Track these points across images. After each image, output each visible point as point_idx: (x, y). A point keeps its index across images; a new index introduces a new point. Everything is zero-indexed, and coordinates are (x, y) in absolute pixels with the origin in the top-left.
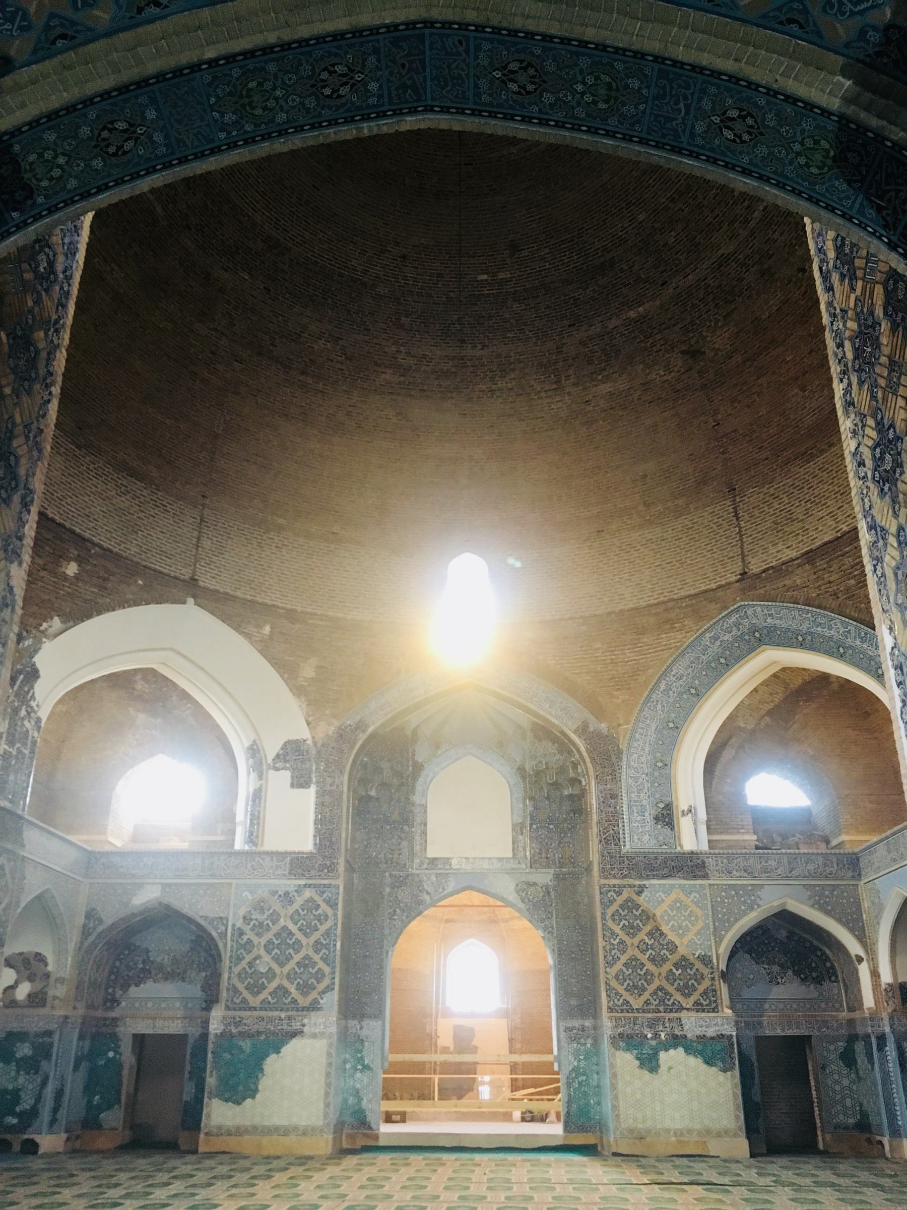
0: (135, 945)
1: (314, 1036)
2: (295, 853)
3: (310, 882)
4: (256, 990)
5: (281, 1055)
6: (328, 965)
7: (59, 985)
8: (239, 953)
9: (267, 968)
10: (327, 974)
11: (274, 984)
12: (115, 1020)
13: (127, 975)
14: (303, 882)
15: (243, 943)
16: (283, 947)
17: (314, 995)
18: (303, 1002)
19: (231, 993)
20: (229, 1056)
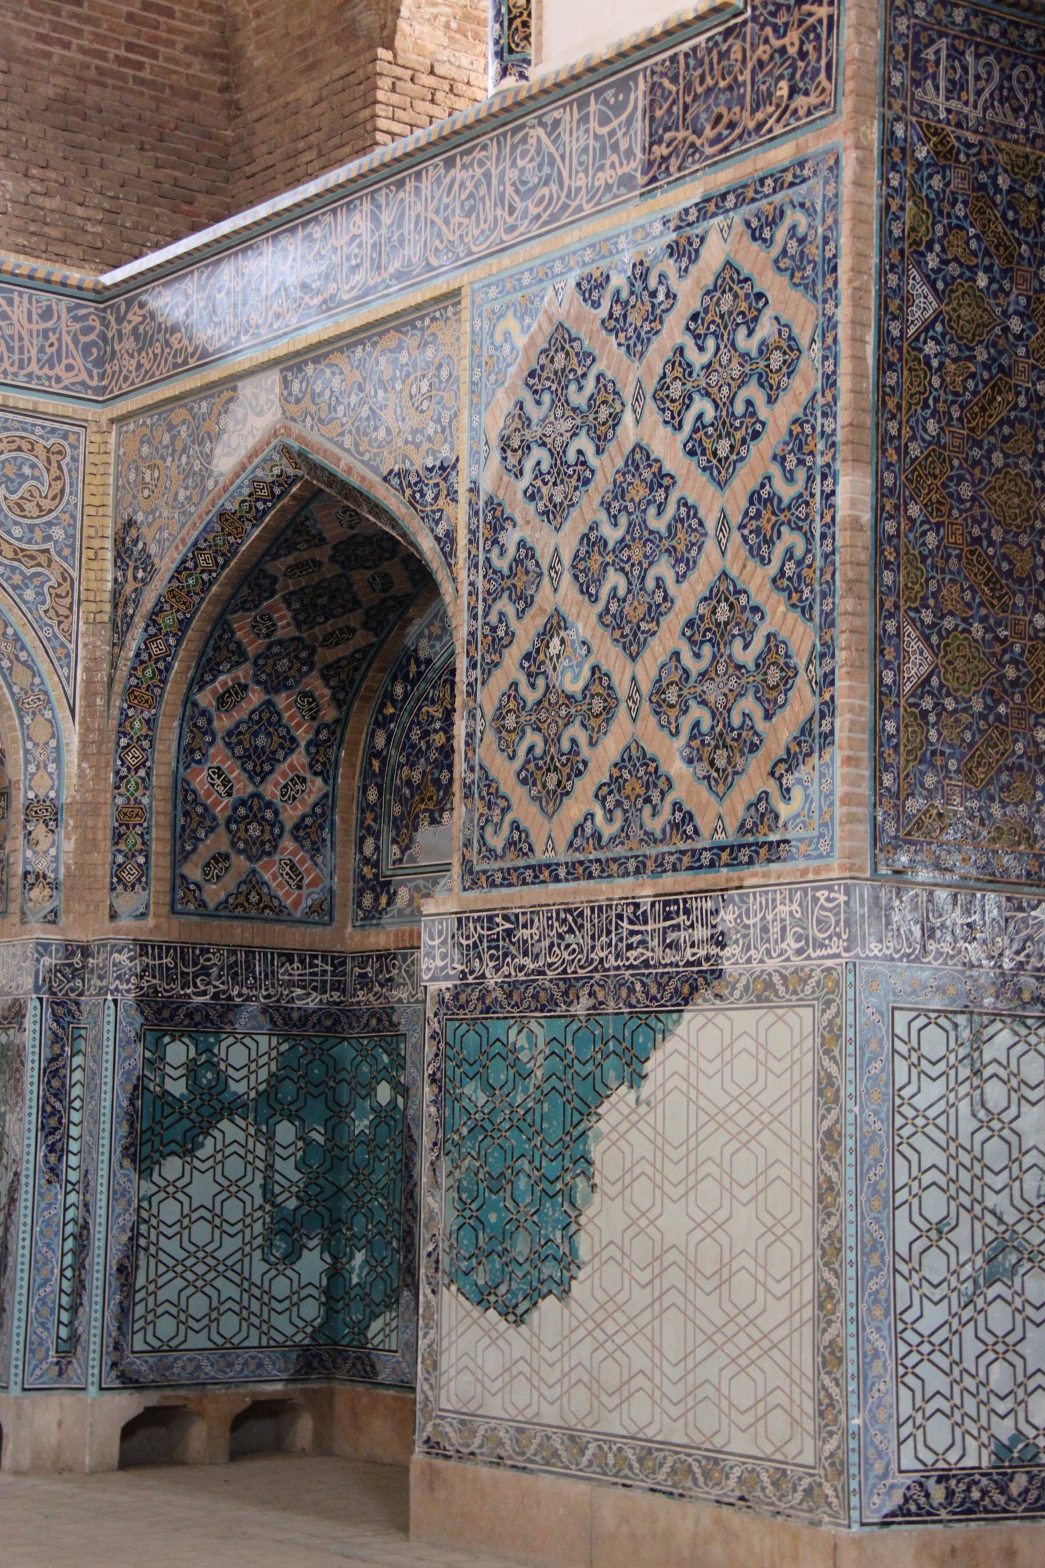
0: (418, 663)
1: (763, 993)
2: (652, 42)
3: (724, 177)
4: (552, 780)
5: (647, 1089)
6: (806, 611)
7: (39, 831)
8: (493, 618)
9: (586, 672)
10: (800, 661)
11: (611, 748)
12: (385, 957)
13: (409, 783)
14: (687, 194)
15: (502, 564)
16: (637, 553)
17: (754, 778)
18: (718, 817)
19: (479, 806)
20: (482, 1098)
